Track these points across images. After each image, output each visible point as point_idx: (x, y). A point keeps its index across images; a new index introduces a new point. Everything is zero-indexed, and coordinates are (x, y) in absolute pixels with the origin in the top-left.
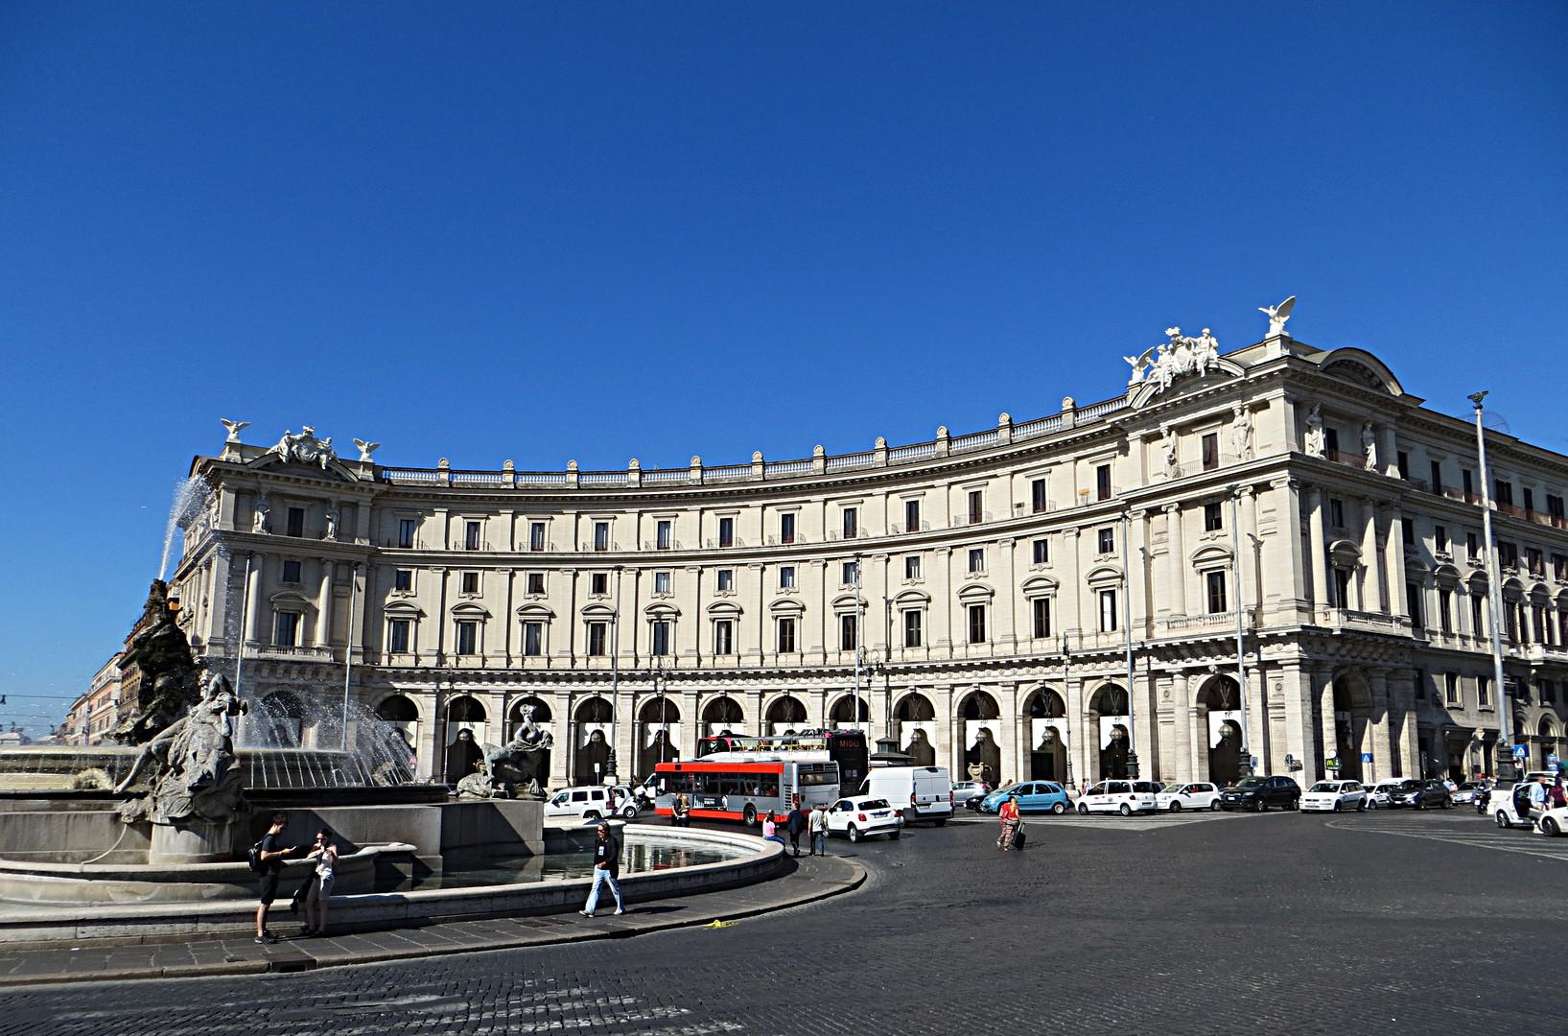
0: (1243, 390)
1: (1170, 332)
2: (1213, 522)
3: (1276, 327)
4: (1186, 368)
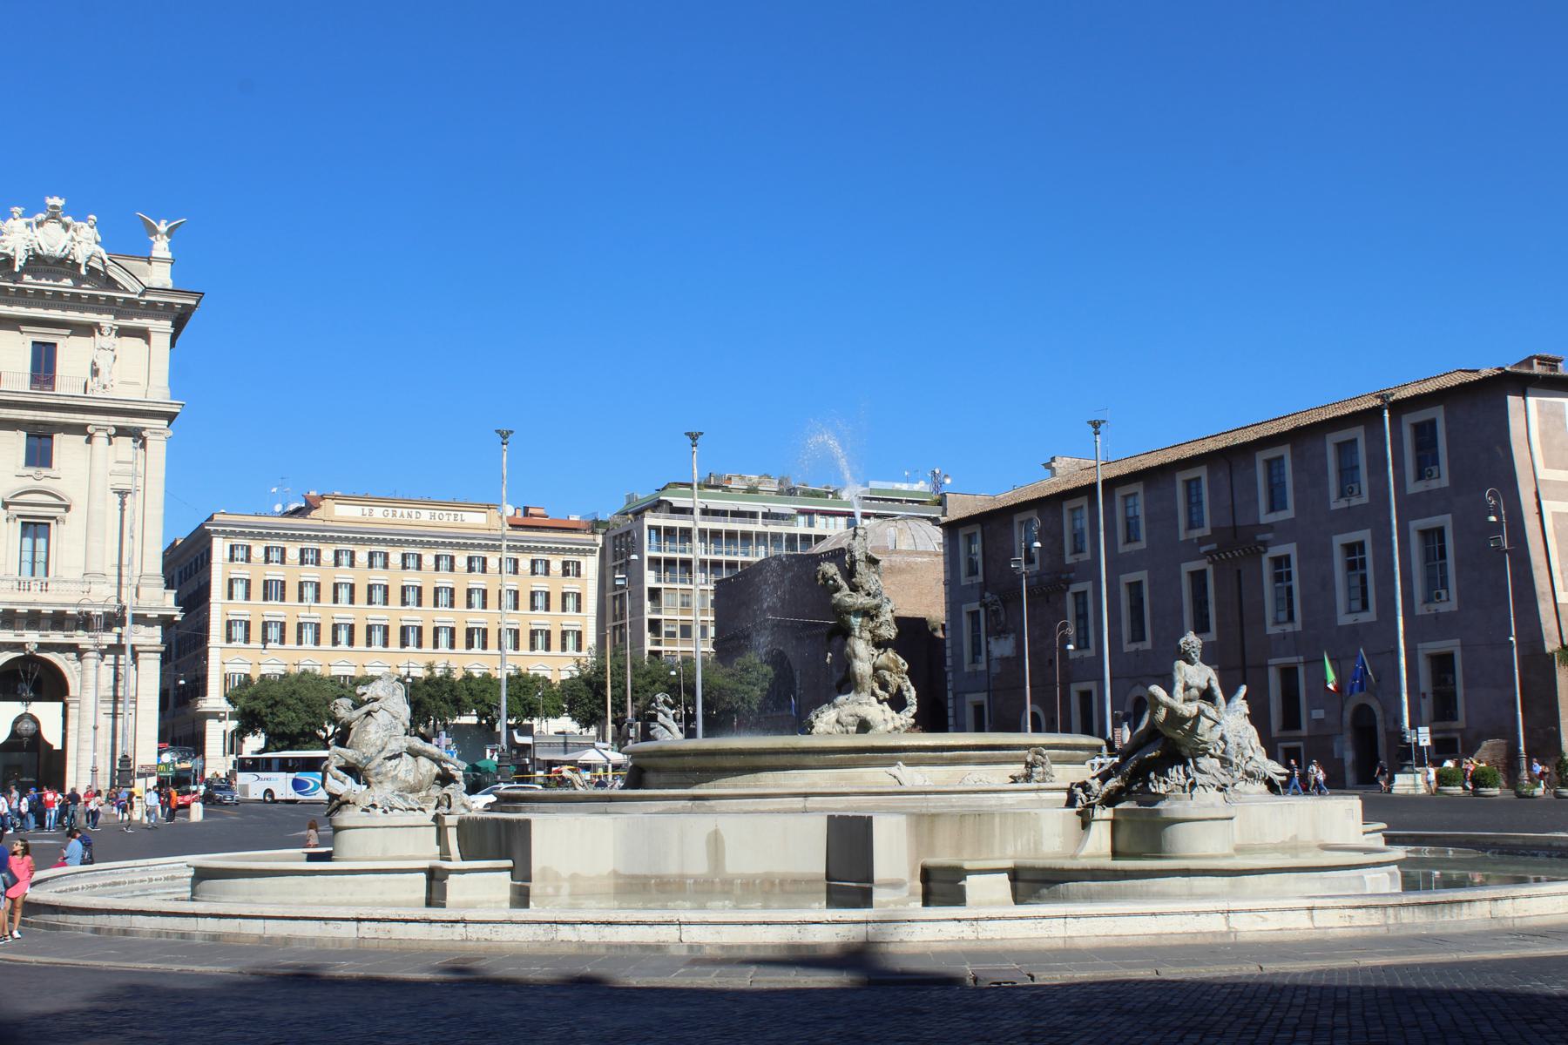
0: (130, 307)
1: (51, 201)
2: (39, 455)
3: (161, 247)
4: (58, 253)
